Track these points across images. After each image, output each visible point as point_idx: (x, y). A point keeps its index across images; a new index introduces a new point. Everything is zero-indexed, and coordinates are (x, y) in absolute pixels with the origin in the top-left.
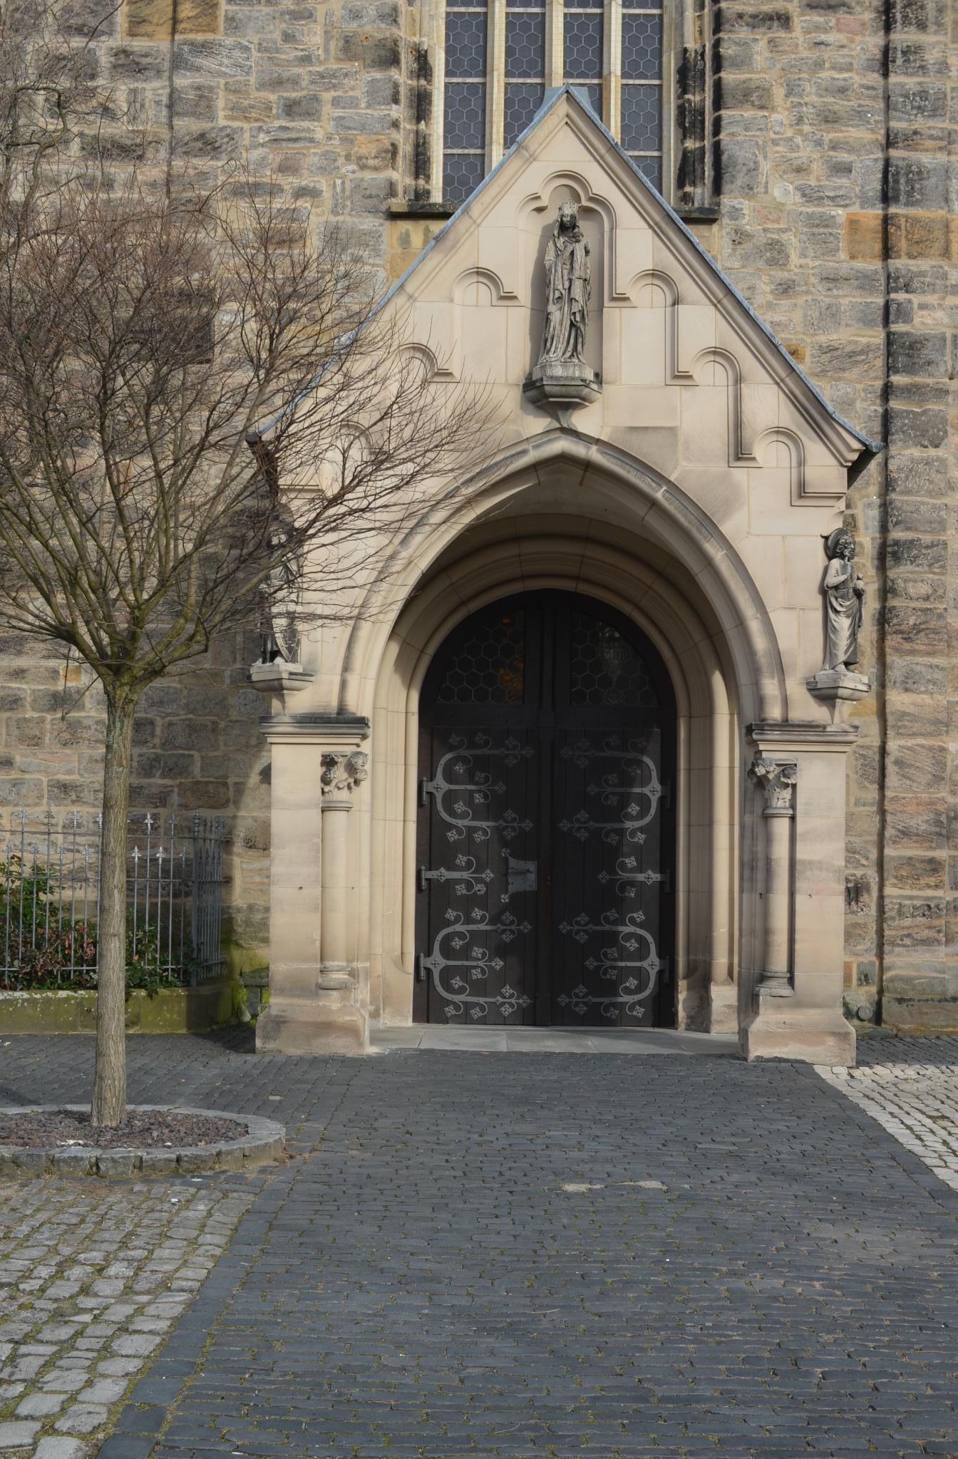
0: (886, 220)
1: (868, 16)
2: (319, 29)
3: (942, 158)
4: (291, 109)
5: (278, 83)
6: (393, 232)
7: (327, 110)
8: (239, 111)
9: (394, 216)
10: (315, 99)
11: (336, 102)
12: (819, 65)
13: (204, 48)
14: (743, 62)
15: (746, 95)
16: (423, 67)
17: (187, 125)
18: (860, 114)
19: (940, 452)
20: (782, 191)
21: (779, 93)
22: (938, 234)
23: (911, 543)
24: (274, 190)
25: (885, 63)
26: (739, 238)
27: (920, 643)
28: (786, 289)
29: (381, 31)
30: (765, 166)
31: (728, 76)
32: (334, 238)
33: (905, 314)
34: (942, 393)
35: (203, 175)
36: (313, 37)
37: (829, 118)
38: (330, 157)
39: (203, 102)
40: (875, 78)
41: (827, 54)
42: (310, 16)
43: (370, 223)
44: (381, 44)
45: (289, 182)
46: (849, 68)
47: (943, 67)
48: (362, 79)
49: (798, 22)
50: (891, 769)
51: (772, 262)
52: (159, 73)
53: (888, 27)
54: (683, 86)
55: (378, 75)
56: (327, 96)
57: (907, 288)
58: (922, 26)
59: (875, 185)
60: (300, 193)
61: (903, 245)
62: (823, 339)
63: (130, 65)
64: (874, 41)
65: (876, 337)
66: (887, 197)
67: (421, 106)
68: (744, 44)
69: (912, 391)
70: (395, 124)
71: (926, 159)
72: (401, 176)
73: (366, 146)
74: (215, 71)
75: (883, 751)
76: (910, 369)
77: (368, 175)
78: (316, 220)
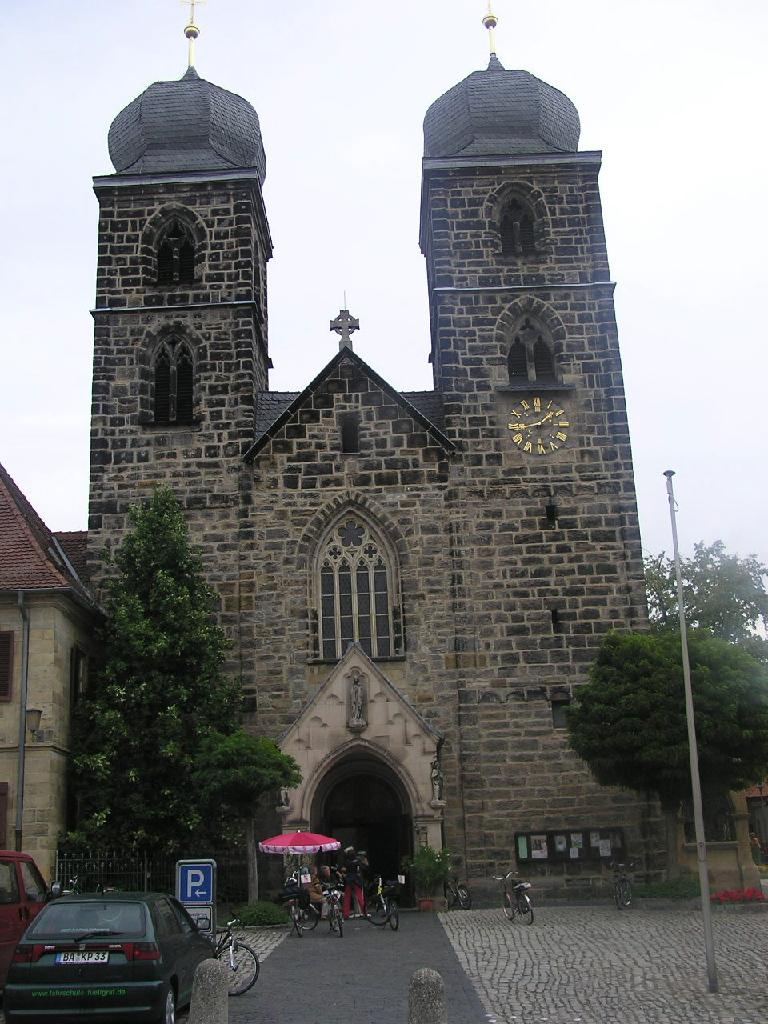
0: (457, 656)
1: (448, 594)
2: (283, 607)
3: (473, 636)
4: (276, 632)
5: (272, 625)
6: (308, 670)
7: (287, 632)
8: (260, 634)
9: (309, 664)
10: (283, 629)
11: (290, 629)
12: (434, 610)
13: (250, 615)
14: (411, 610)
15: (412, 619)
16: (316, 616)
17: (245, 638)
18: (447, 624)
19: (477, 726)
20: (425, 649)
21: (422, 619)
22: (473, 659)
23: (469, 755)
24: (273, 657)
25: (453, 607)
26: (413, 664)
27: (473, 785)
28: (427, 679)
29: (302, 608)
30: (419, 642)
31: (407, 615)
32: (292, 672)
33: (463, 684)
34: (475, 708)
35: (251, 655)
36: (282, 610)
37: (438, 626)
38: (289, 647)
39: (249, 631)
40: (451, 612)
41: (436, 607)
42: (281, 603)
43: (300, 667)
44: (302, 611)
45: (277, 656)
46: (443, 610)
47: (472, 608)
48: (297, 622)
49: (428, 596)
50: (467, 824)
51: (423, 672)
52: (235, 622)
53: (454, 596)
54: (395, 618)
55: (301, 621)
56: (287, 628)
57: (464, 677)
58: (464, 596)
59: (452, 648)
60: (280, 658)
61: (461, 664)
62: (440, 694)
63: (226, 620)
64: (449, 601)
65: (456, 692)
66: (456, 648)
67: (315, 628)
68: (411, 605)
69: (467, 709)
70: (308, 635)
71: (467, 637)
72: (310, 651)
73: (299, 642)
74: (253, 622)
75: (464, 818)
76: (465, 702)
77: (300, 652)
78: (285, 666)
